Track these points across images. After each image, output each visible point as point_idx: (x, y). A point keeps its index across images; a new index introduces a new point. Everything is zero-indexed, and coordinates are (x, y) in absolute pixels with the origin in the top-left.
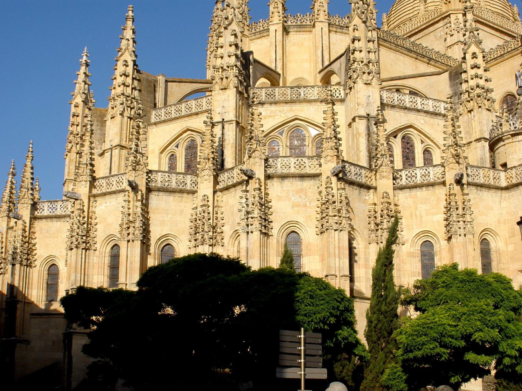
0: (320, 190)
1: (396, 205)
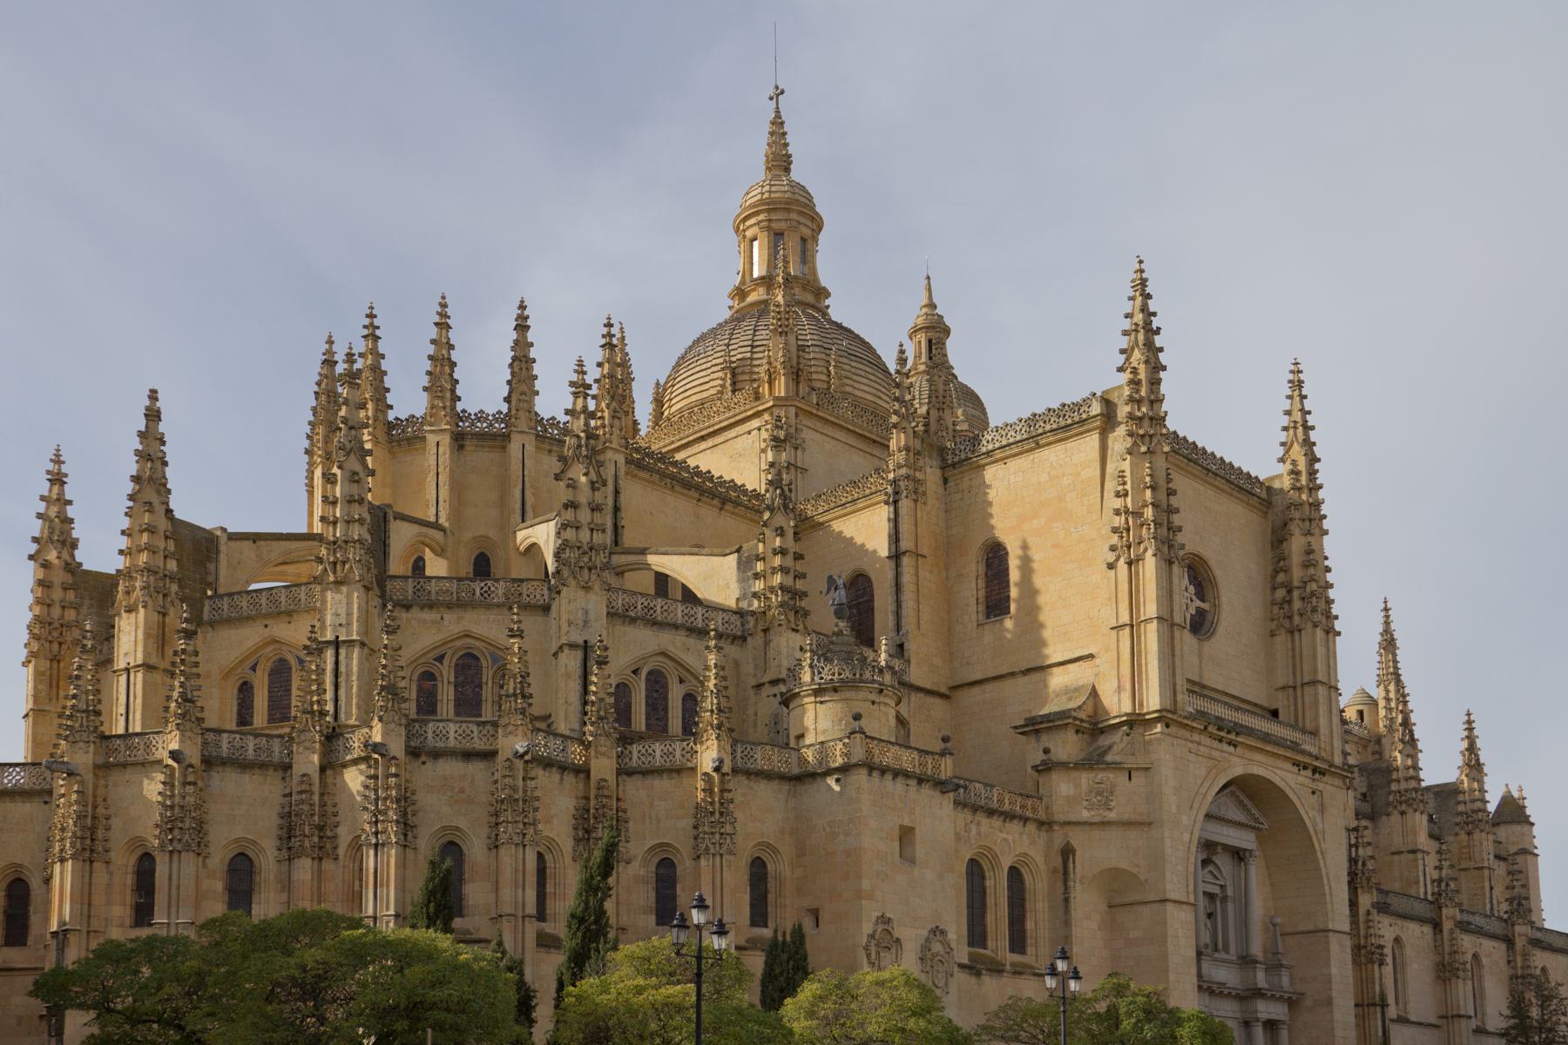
0: (495, 778)
1: (618, 799)
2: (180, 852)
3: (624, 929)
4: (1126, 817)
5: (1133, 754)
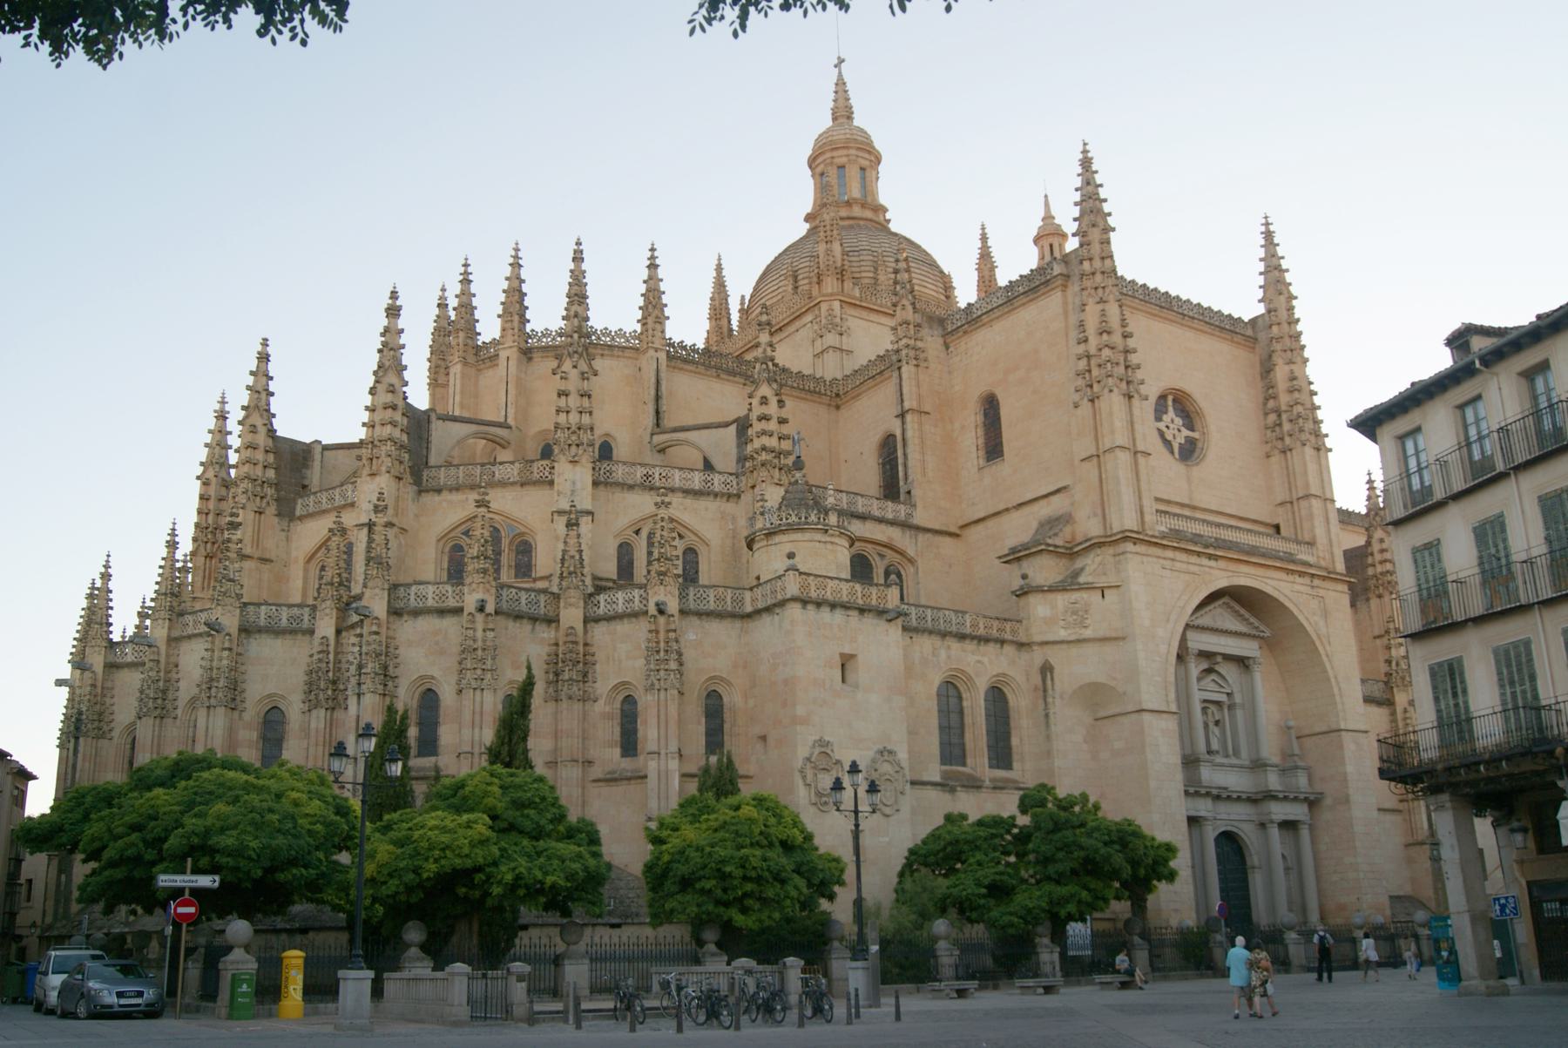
1: (586, 644)
3: (590, 762)
4: (1100, 634)
5: (1105, 574)
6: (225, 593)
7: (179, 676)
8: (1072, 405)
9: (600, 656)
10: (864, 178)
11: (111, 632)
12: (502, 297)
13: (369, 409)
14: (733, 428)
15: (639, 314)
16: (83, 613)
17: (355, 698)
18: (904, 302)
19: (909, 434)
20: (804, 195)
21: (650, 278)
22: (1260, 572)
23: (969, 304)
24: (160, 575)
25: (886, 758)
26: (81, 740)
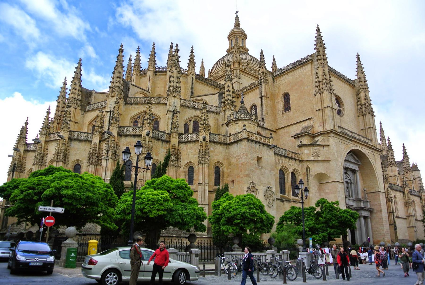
2: (59, 162)
4: (323, 159)
6: (65, 127)
7: (48, 153)
8: (314, 95)
9: (182, 154)
10: (243, 42)
11: (27, 141)
12: (149, 57)
13: (113, 78)
14: (218, 94)
15: (188, 65)
16: (19, 136)
17: (106, 161)
18: (263, 67)
19: (264, 102)
20: (226, 45)
21: (191, 55)
22: (361, 146)
23: (281, 68)
24: (44, 121)
25: (269, 189)
26: (15, 173)
